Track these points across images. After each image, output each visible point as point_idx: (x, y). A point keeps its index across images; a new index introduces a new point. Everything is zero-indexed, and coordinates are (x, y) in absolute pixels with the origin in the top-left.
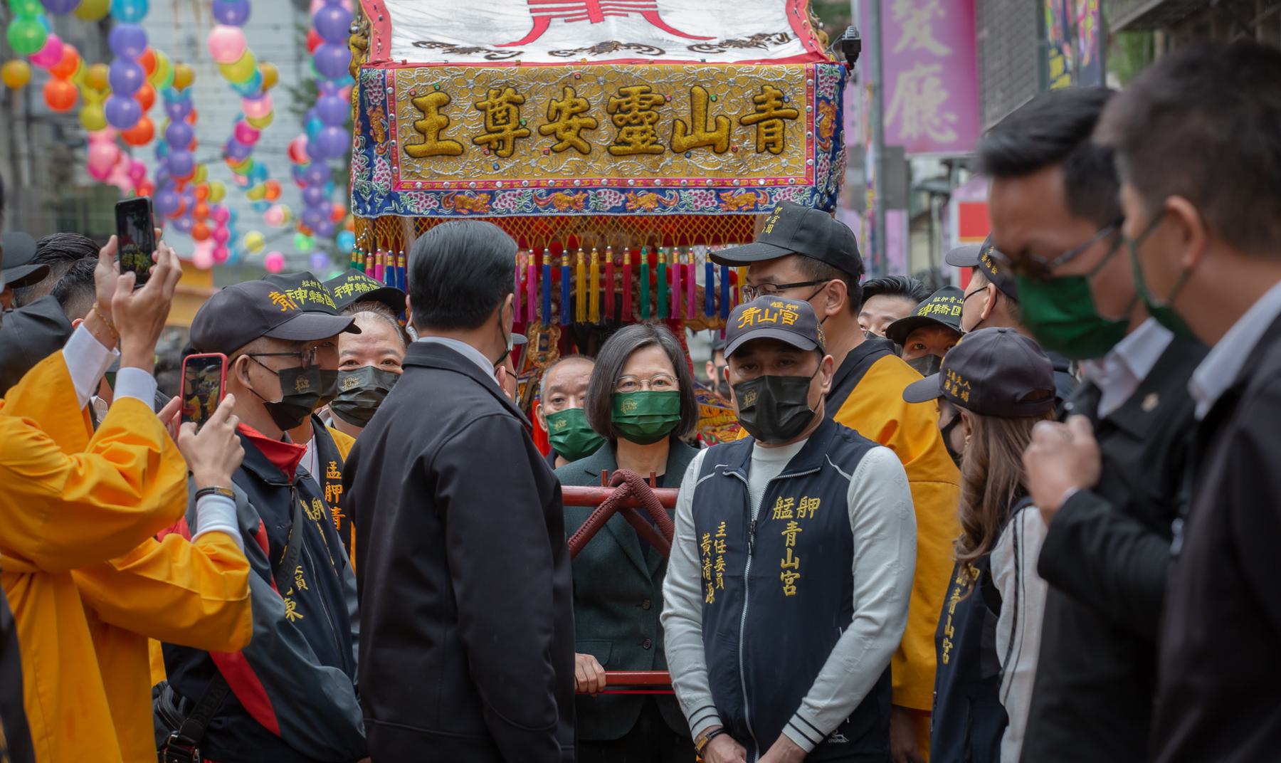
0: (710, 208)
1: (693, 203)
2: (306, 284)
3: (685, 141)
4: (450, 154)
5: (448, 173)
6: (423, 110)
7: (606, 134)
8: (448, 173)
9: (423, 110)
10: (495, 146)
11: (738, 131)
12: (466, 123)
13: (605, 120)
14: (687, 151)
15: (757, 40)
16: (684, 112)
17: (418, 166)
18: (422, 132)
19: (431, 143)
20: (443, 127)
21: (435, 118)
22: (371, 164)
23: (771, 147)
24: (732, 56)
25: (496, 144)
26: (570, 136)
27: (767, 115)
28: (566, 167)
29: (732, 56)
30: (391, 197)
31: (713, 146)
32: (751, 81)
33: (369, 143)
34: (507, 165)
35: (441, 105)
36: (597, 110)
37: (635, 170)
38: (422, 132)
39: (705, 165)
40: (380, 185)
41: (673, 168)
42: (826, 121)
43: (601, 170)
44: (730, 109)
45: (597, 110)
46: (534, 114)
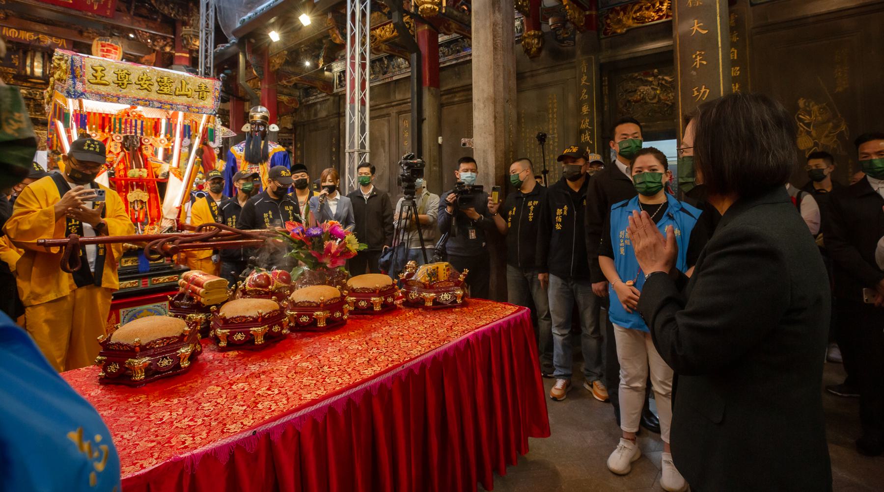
3: (177, 93)
6: (96, 71)
7: (156, 87)
10: (120, 85)
12: (110, 77)
13: (156, 84)
18: (96, 77)
19: (98, 81)
22: (75, 84)
26: (145, 86)
31: (186, 95)
34: (124, 91)
36: (154, 81)
38: (96, 77)
39: (184, 100)
43: (154, 96)
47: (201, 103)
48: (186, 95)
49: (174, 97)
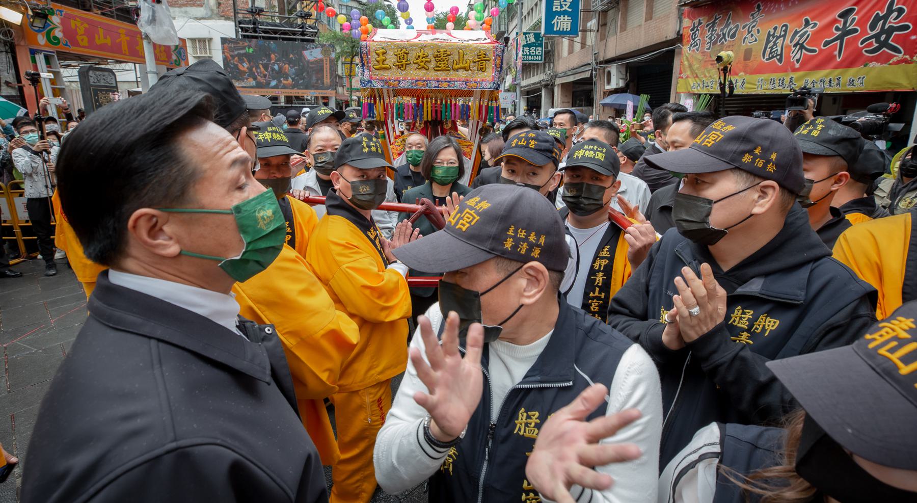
0: (464, 88)
1: (458, 86)
2: (269, 129)
4: (386, 69)
5: (387, 75)
7: (433, 63)
8: (387, 75)
9: (378, 55)
10: (400, 67)
11: (472, 64)
12: (391, 59)
14: (457, 70)
15: (478, 40)
16: (457, 58)
17: (377, 72)
19: (381, 65)
20: (384, 60)
21: (382, 57)
23: (482, 69)
24: (471, 42)
25: (401, 66)
26: (422, 64)
27: (481, 60)
28: (421, 74)
29: (471, 42)
30: (369, 81)
31: (465, 68)
32: (476, 49)
33: (363, 65)
35: (384, 53)
36: (431, 57)
37: (441, 75)
39: (462, 74)
40: (366, 78)
41: (453, 75)
42: (498, 62)
43: (432, 75)
44: (470, 57)
45: (431, 57)
46: (412, 57)
47: (479, 76)
48: (465, 68)
49: (452, 72)
